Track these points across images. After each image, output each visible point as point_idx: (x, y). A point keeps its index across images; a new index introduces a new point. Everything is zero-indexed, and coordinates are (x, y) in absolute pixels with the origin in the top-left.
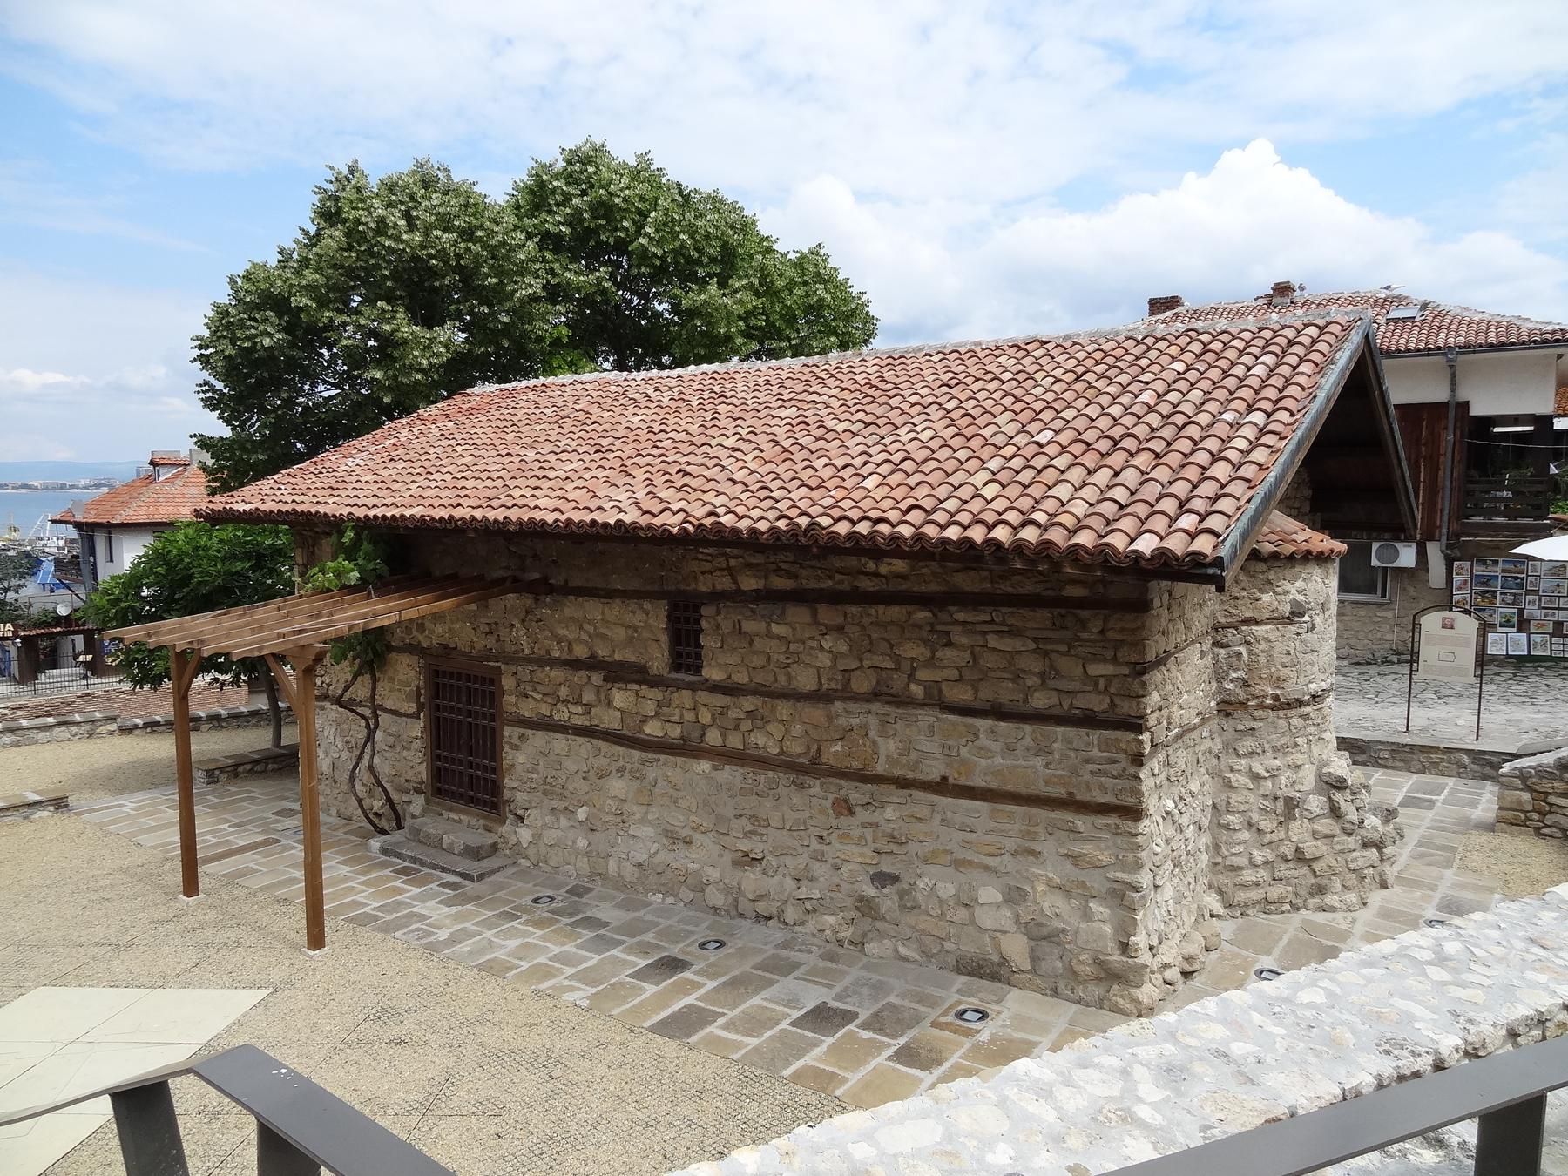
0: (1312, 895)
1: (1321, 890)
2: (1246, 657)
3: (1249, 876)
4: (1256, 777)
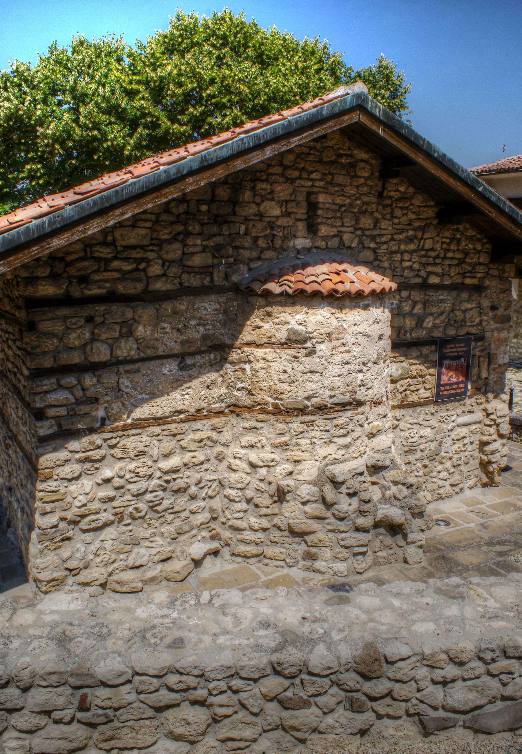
0: (304, 559)
1: (310, 557)
2: (249, 372)
3: (248, 535)
4: (253, 466)
